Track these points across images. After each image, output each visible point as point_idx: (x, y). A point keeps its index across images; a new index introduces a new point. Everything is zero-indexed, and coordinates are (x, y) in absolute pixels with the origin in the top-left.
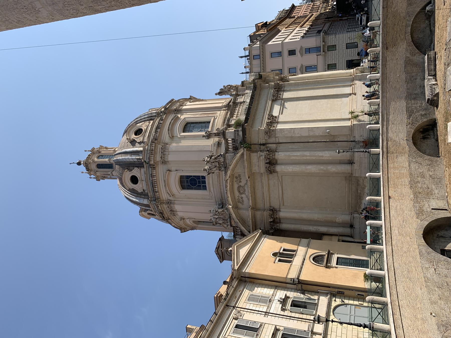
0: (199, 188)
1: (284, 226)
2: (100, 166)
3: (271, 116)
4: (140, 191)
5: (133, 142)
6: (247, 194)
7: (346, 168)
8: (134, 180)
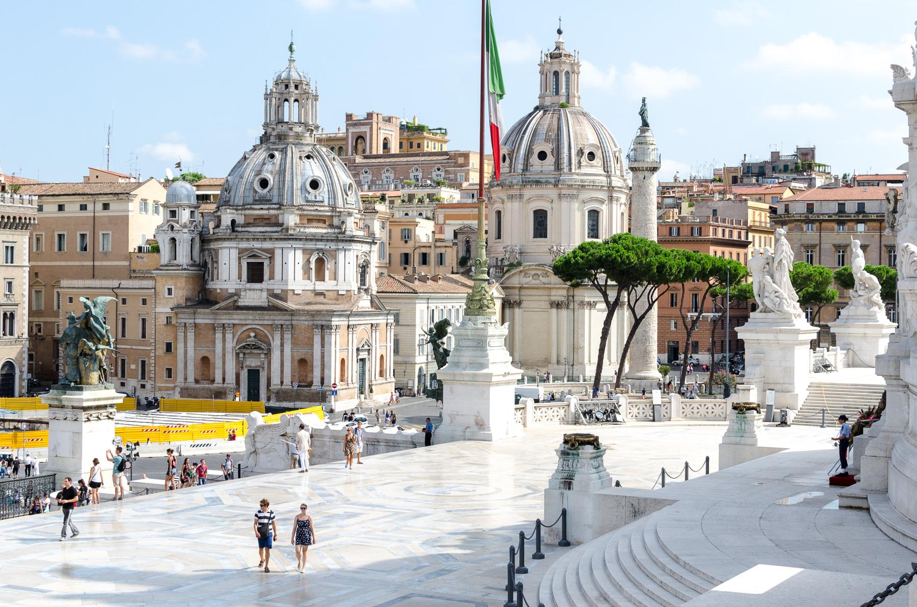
0: (536, 229)
1: (507, 311)
2: (556, 74)
3: (595, 303)
4: (531, 160)
5: (581, 152)
6: (534, 282)
7: (554, 360)
8: (542, 156)
